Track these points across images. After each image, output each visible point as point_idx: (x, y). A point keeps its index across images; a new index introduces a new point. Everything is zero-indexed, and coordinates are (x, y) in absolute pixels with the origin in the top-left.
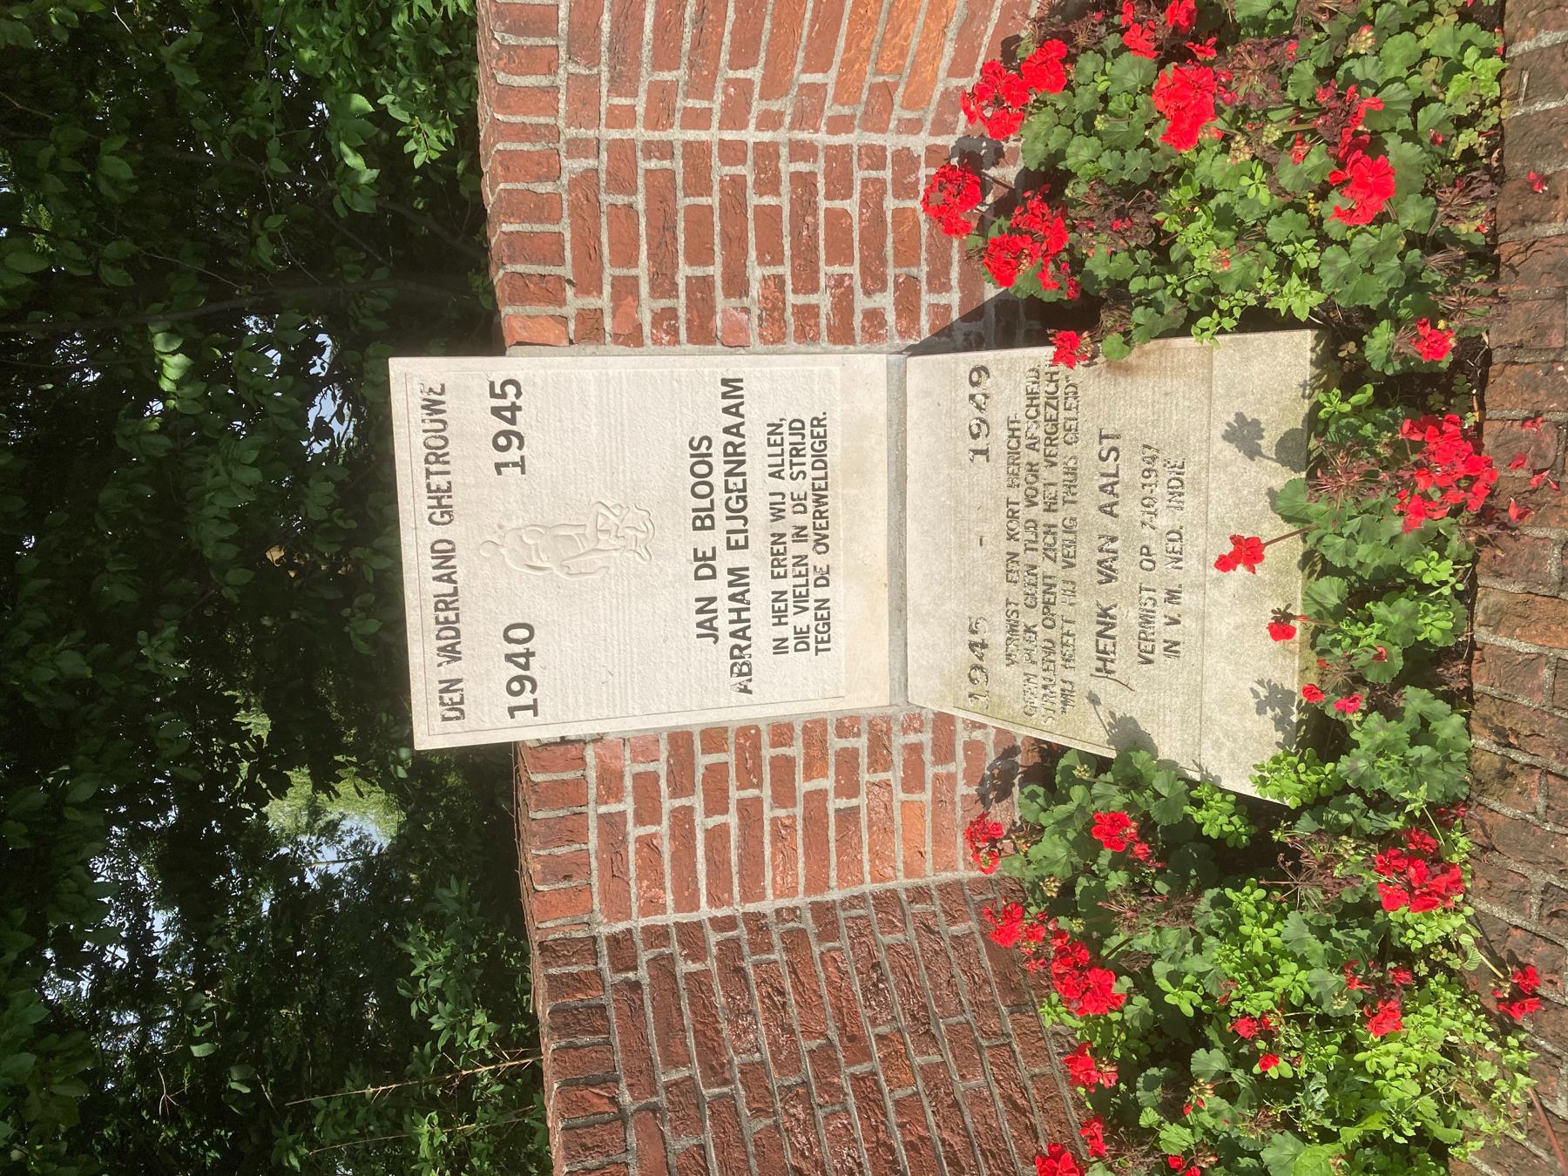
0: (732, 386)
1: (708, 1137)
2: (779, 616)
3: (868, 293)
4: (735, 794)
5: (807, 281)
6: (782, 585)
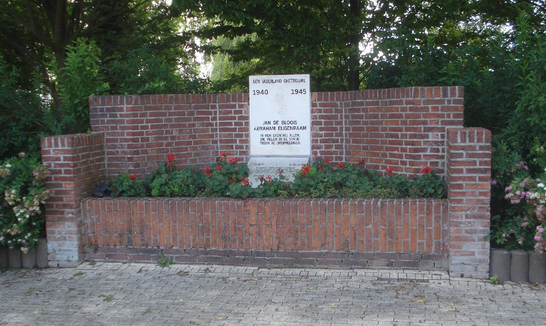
0: (305, 128)
1: (186, 116)
2: (266, 135)
3: (320, 152)
4: (237, 127)
5: (322, 141)
6: (272, 136)
